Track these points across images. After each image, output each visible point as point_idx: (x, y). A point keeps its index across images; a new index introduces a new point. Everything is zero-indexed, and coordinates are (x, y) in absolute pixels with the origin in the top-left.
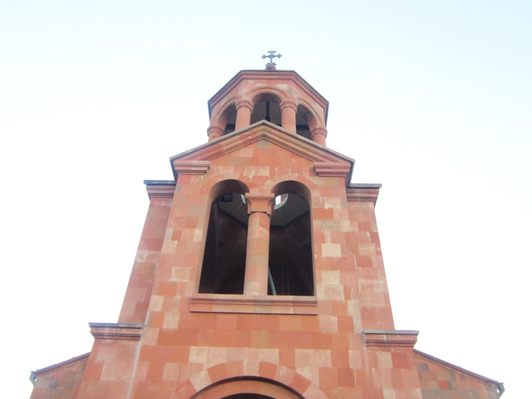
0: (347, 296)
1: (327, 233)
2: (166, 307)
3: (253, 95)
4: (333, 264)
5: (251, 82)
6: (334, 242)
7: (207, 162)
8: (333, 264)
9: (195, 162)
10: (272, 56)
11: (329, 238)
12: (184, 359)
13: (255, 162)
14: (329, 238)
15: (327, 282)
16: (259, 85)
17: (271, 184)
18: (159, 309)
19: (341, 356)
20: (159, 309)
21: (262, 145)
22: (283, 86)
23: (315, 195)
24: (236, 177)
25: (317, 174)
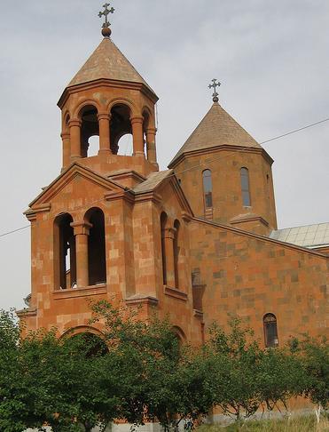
0: (120, 281)
1: (112, 242)
2: (44, 298)
3: (78, 109)
4: (116, 263)
5: (75, 95)
6: (115, 248)
7: (47, 204)
8: (116, 263)
9: (42, 205)
10: (106, 12)
11: (113, 247)
12: (55, 322)
13: (74, 196)
14: (113, 247)
15: (113, 273)
16: (81, 98)
17: (84, 211)
18: (41, 300)
19: (115, 313)
20: (41, 300)
21: (78, 178)
22: (97, 96)
23: (106, 215)
24: (66, 211)
25: (107, 200)
